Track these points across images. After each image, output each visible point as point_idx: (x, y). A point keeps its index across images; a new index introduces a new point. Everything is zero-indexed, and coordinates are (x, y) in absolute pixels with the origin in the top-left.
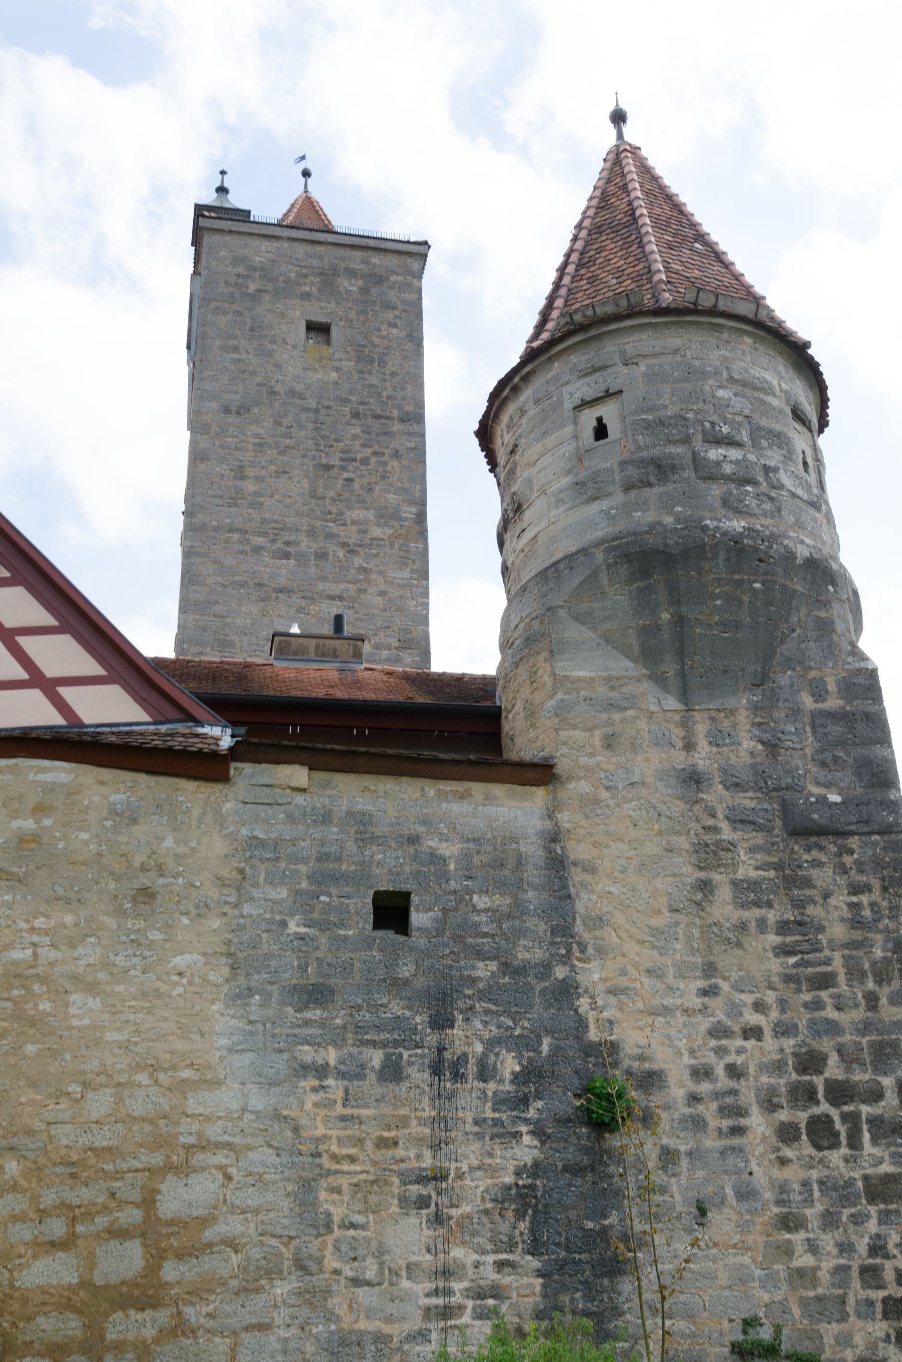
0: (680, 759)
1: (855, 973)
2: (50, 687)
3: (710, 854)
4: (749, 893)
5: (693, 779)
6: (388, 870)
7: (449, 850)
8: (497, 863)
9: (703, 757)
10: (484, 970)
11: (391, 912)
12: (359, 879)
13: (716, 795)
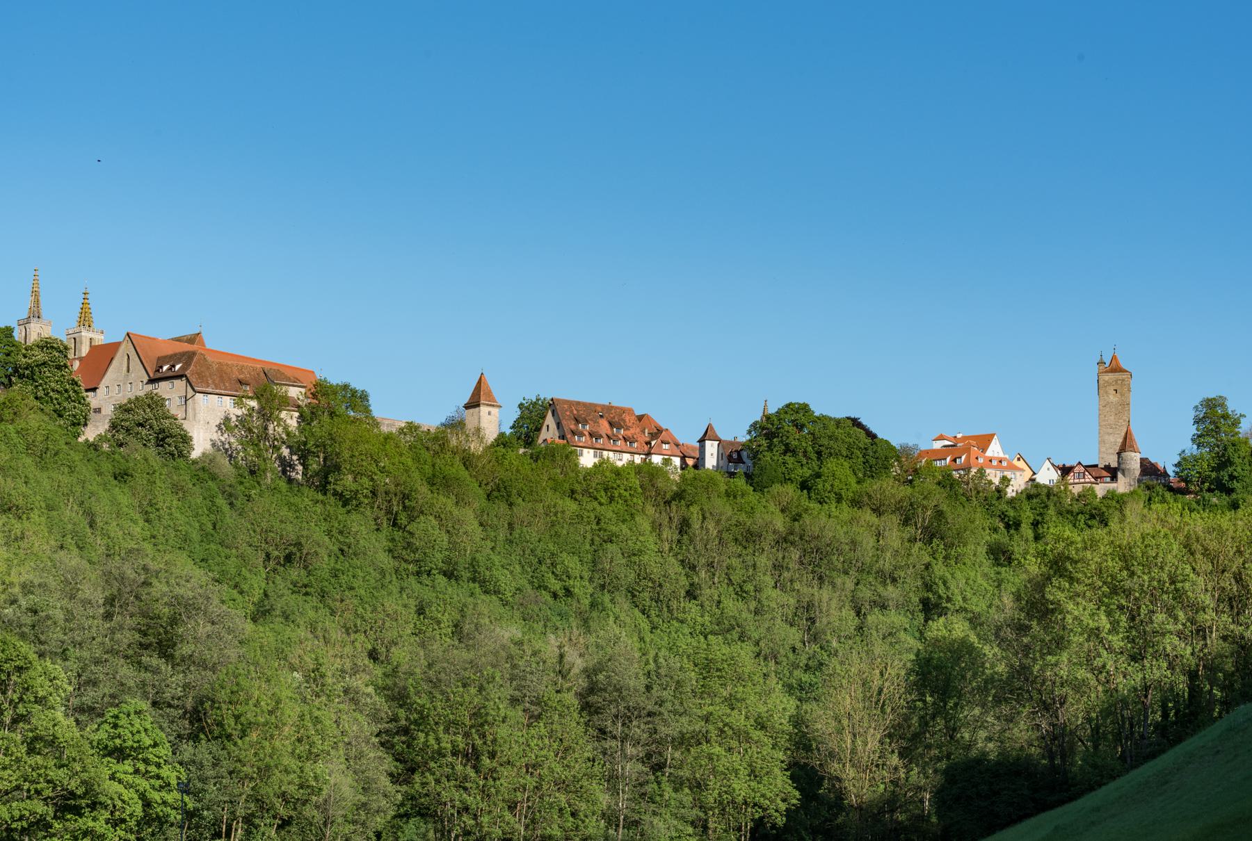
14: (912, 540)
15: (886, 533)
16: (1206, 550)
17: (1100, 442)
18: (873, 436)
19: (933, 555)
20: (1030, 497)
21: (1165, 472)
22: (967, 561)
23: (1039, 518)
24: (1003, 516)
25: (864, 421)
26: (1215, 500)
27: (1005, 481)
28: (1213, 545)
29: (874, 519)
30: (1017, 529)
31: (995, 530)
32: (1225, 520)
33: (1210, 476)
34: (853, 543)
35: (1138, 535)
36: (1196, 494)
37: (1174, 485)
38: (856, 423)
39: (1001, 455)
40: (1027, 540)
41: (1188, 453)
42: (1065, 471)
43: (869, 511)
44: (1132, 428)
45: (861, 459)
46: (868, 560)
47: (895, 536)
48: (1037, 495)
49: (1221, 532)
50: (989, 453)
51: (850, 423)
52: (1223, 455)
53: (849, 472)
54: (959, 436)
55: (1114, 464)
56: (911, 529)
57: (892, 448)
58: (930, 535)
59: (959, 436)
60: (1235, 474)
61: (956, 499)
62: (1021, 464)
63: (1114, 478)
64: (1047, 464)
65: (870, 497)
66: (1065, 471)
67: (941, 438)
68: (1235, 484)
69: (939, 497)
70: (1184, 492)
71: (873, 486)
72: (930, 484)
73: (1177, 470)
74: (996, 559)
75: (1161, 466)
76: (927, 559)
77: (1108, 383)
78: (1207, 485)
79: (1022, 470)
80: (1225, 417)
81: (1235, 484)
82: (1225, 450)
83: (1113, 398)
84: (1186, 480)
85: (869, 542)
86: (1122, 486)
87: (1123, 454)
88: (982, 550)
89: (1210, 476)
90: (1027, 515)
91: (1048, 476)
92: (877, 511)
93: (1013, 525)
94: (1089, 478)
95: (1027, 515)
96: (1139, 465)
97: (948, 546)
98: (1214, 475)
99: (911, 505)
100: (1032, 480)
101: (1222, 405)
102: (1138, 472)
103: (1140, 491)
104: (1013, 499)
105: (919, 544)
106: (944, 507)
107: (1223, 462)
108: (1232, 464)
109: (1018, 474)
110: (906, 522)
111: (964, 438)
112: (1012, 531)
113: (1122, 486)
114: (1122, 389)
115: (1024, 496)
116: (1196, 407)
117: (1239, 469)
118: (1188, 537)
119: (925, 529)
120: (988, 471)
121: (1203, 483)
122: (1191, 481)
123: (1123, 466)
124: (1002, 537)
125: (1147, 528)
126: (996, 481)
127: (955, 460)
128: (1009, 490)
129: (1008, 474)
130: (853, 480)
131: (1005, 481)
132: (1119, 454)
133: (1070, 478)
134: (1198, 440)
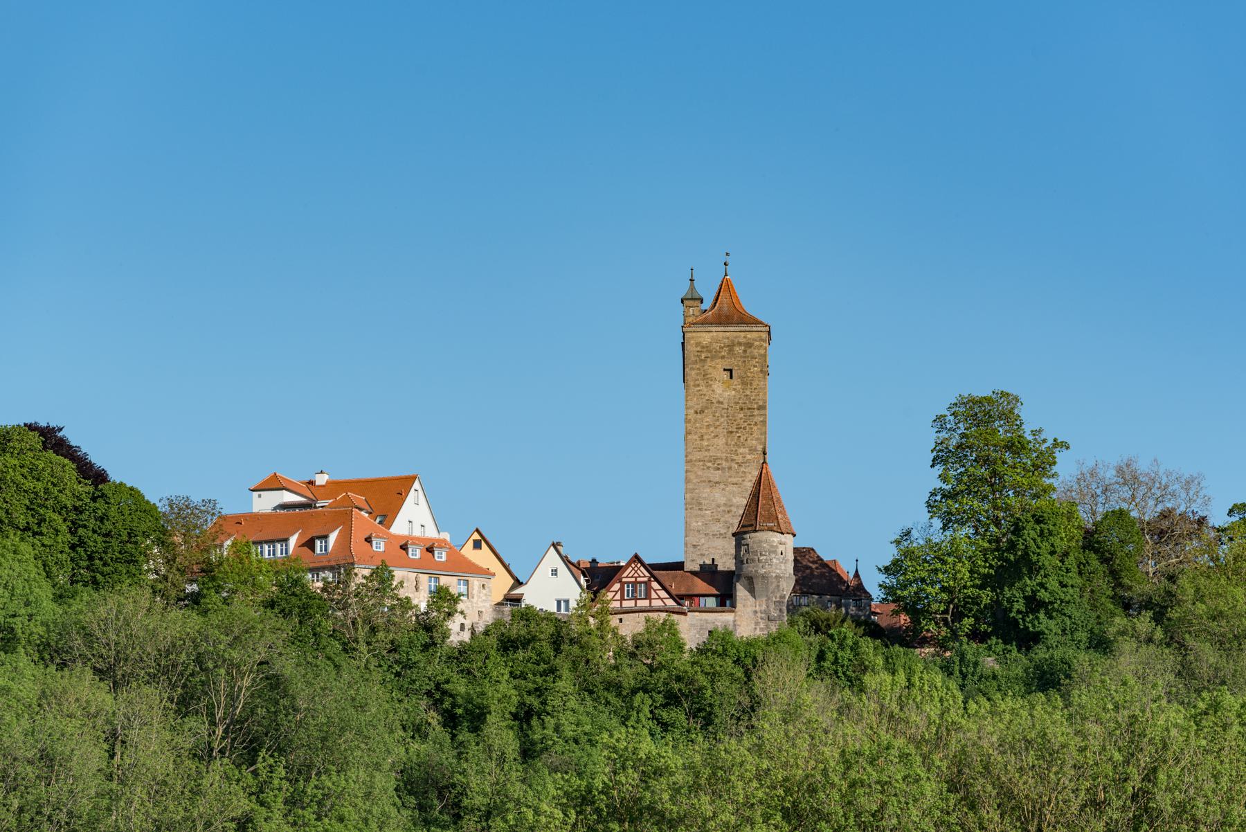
3: (757, 623)
5: (756, 612)
6: (711, 627)
9: (758, 608)
13: (759, 615)
14: (203, 754)
15: (134, 735)
16: (1010, 795)
17: (688, 506)
18: (99, 477)
19: (258, 795)
20: (508, 645)
21: (860, 587)
22: (347, 811)
23: (533, 701)
24: (438, 694)
25: (73, 436)
26: (990, 663)
27: (444, 599)
28: (1026, 786)
29: (102, 697)
30: (475, 729)
31: (418, 731)
32: (1046, 715)
33: (975, 600)
34: (46, 758)
35: (831, 753)
36: (942, 645)
37: (884, 621)
38: (51, 439)
39: (431, 533)
40: (502, 759)
41: (918, 539)
42: (598, 577)
43: (89, 674)
44: (773, 469)
45: (65, 537)
46: (85, 806)
47: (156, 744)
48: (526, 642)
49: (1050, 754)
50: (399, 527)
51: (35, 440)
52: (1012, 546)
53: (34, 570)
54: (321, 480)
55: (726, 563)
56: (197, 724)
57: (147, 509)
58: (248, 744)
59: (321, 480)
60: (1043, 595)
61: (318, 646)
62: (483, 558)
63: (726, 599)
64: (552, 559)
65: (88, 636)
66: (598, 577)
67: (273, 484)
68: (1043, 622)
69: (271, 640)
70: (910, 639)
71: (98, 609)
72: (246, 608)
73: (890, 581)
74: (421, 807)
75: (846, 569)
76: (242, 804)
77: (710, 352)
78: (968, 622)
79: (488, 574)
80: (1016, 446)
81: (1043, 622)
82: (1017, 530)
83: (722, 390)
84: (915, 610)
85: (88, 757)
86: (747, 620)
87: (752, 538)
88: (386, 782)
89: (975, 600)
90: (501, 693)
91: (552, 590)
92: (110, 674)
93: (463, 718)
94: (660, 598)
95: (501, 693)
96: (790, 567)
97: (305, 770)
98: (986, 596)
99: (199, 660)
100: (514, 600)
101: (1009, 416)
102: (787, 586)
103: (794, 635)
104: (461, 654)
105: (220, 765)
106: (287, 666)
107: (1010, 564)
108: (1033, 568)
109: (476, 583)
110: (184, 705)
111: (335, 487)
112: (464, 736)
113: (747, 620)
114: (747, 367)
115: (493, 640)
116: (940, 419)
117: (1053, 583)
118: (960, 762)
119: (236, 726)
120: (399, 574)
121: (958, 616)
122: (926, 612)
123: (749, 569)
124: (434, 748)
125: (855, 735)
126: (421, 601)
127: (310, 544)
128: (454, 625)
129: (453, 584)
130: (44, 592)
131: (444, 599)
132: (739, 536)
133: (612, 595)
134: (944, 505)
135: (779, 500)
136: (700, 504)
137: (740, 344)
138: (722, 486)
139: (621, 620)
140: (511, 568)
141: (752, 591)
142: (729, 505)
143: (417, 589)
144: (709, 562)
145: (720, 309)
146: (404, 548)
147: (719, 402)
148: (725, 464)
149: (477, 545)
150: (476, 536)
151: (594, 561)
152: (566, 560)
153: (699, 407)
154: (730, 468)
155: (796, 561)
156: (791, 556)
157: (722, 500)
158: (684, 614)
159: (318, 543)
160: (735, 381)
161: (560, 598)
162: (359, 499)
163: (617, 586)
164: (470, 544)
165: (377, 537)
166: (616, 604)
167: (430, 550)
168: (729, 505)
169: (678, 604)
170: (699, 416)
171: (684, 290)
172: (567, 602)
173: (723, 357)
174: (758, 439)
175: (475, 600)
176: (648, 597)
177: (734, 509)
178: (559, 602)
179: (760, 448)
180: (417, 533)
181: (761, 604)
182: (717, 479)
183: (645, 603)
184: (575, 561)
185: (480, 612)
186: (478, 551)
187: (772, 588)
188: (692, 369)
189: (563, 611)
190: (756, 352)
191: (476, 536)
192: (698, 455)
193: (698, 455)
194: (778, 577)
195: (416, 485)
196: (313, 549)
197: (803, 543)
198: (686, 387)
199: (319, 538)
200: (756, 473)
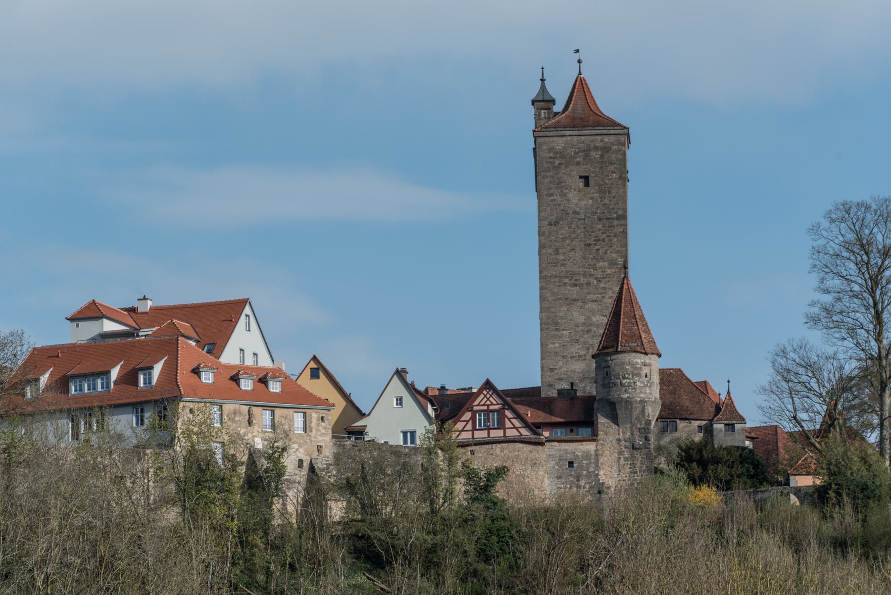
0: (617, 436)
1: (640, 471)
2: (517, 428)
3: (621, 453)
4: (626, 459)
5: (619, 440)
6: (570, 457)
7: (579, 454)
8: (587, 456)
9: (621, 436)
10: (585, 472)
11: (571, 464)
12: (565, 460)
13: (623, 443)
39: (265, 362)
42: (448, 406)
50: (229, 356)
55: (587, 388)
62: (321, 388)
64: (397, 388)
79: (325, 404)
83: (577, 199)
111: (161, 313)
135: (642, 317)
136: (557, 324)
137: (596, 148)
138: (580, 304)
139: (473, 453)
140: (353, 398)
141: (615, 419)
142: (588, 324)
143: (250, 423)
144: (565, 386)
145: (574, 111)
146: (235, 379)
147: (575, 213)
148: (583, 280)
149: (314, 374)
150: (313, 365)
151: (443, 388)
152: (411, 388)
153: (553, 218)
154: (588, 284)
155: (662, 382)
156: (656, 379)
157: (581, 319)
158: (541, 444)
159: (141, 378)
160: (592, 190)
161: (406, 429)
162: (183, 325)
163: (468, 415)
164: (308, 372)
165: (206, 367)
166: (466, 436)
167: (263, 381)
168: (588, 324)
169: (535, 433)
170: (553, 228)
171: (534, 91)
172: (413, 433)
173: (578, 163)
174: (617, 252)
175: (313, 434)
176: (501, 426)
177: (594, 329)
178: (405, 434)
179: (620, 261)
180: (249, 362)
181: (624, 433)
182: (575, 296)
183: (499, 433)
184: (421, 388)
185: (319, 448)
186: (315, 381)
187: (636, 413)
188: (545, 177)
189: (409, 445)
190: (613, 157)
191: (313, 365)
192: (554, 271)
193: (554, 271)
194: (643, 402)
195: (247, 310)
196: (136, 383)
197: (668, 362)
198: (539, 197)
199: (142, 369)
200: (617, 289)
